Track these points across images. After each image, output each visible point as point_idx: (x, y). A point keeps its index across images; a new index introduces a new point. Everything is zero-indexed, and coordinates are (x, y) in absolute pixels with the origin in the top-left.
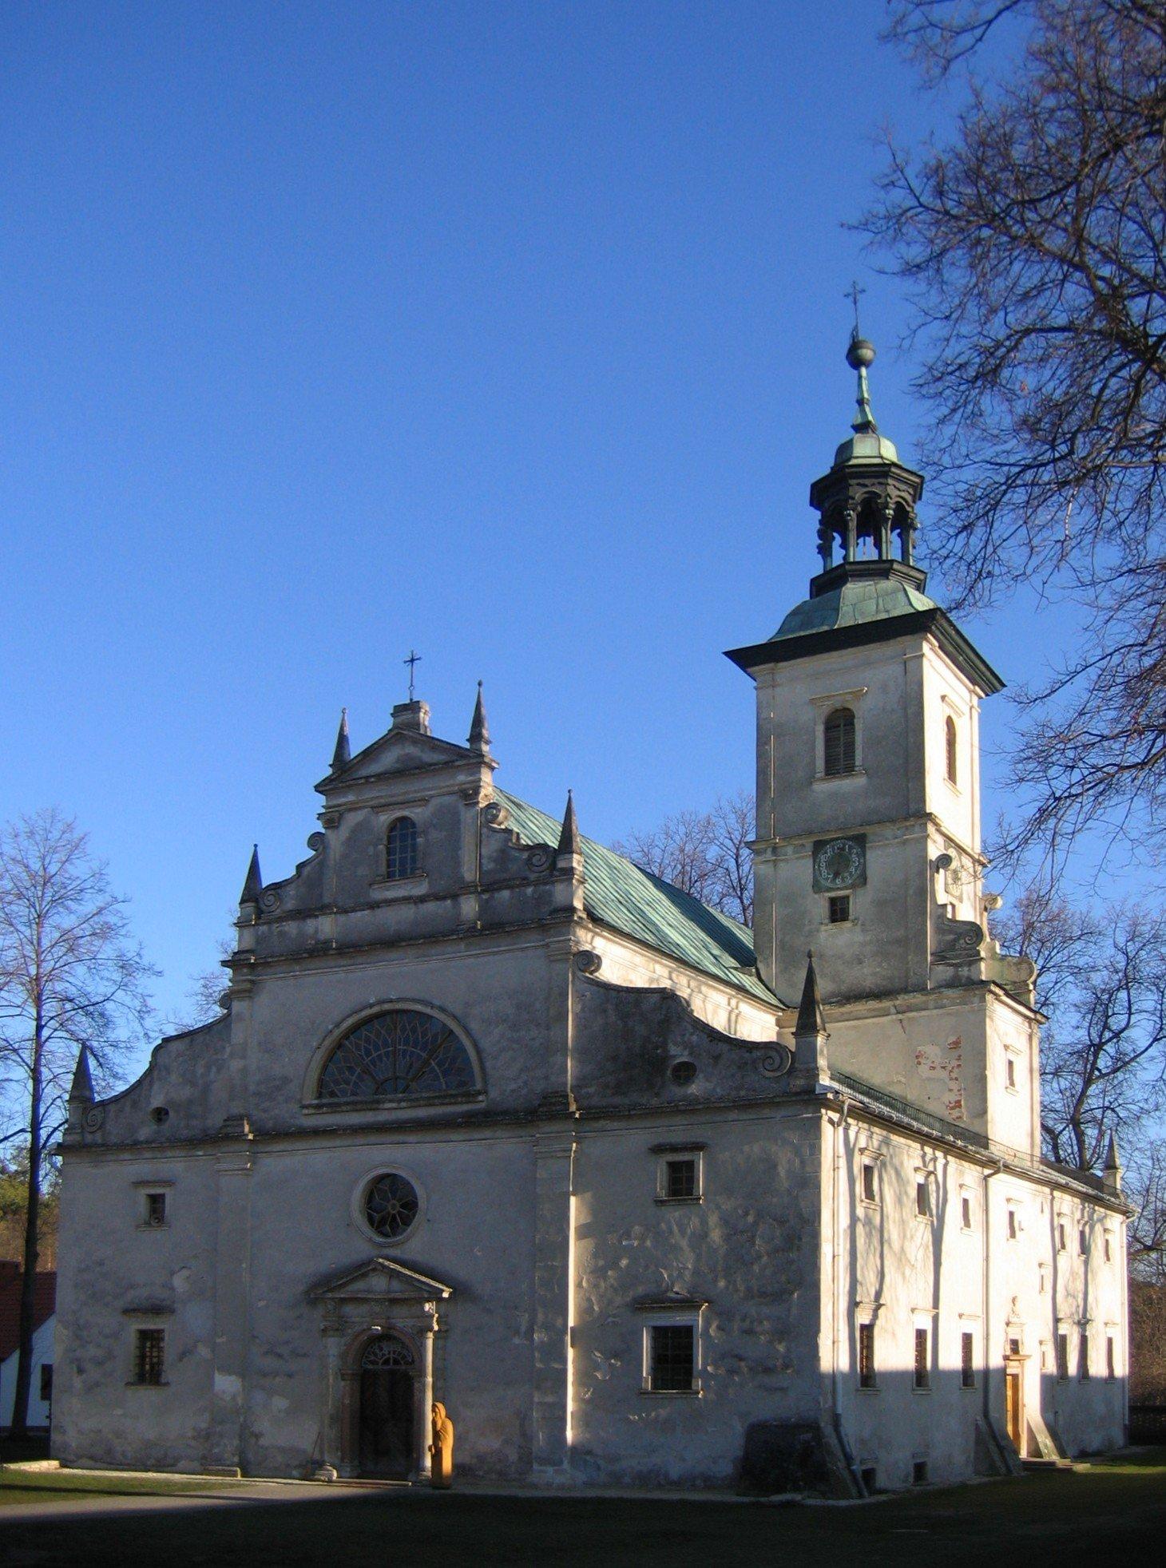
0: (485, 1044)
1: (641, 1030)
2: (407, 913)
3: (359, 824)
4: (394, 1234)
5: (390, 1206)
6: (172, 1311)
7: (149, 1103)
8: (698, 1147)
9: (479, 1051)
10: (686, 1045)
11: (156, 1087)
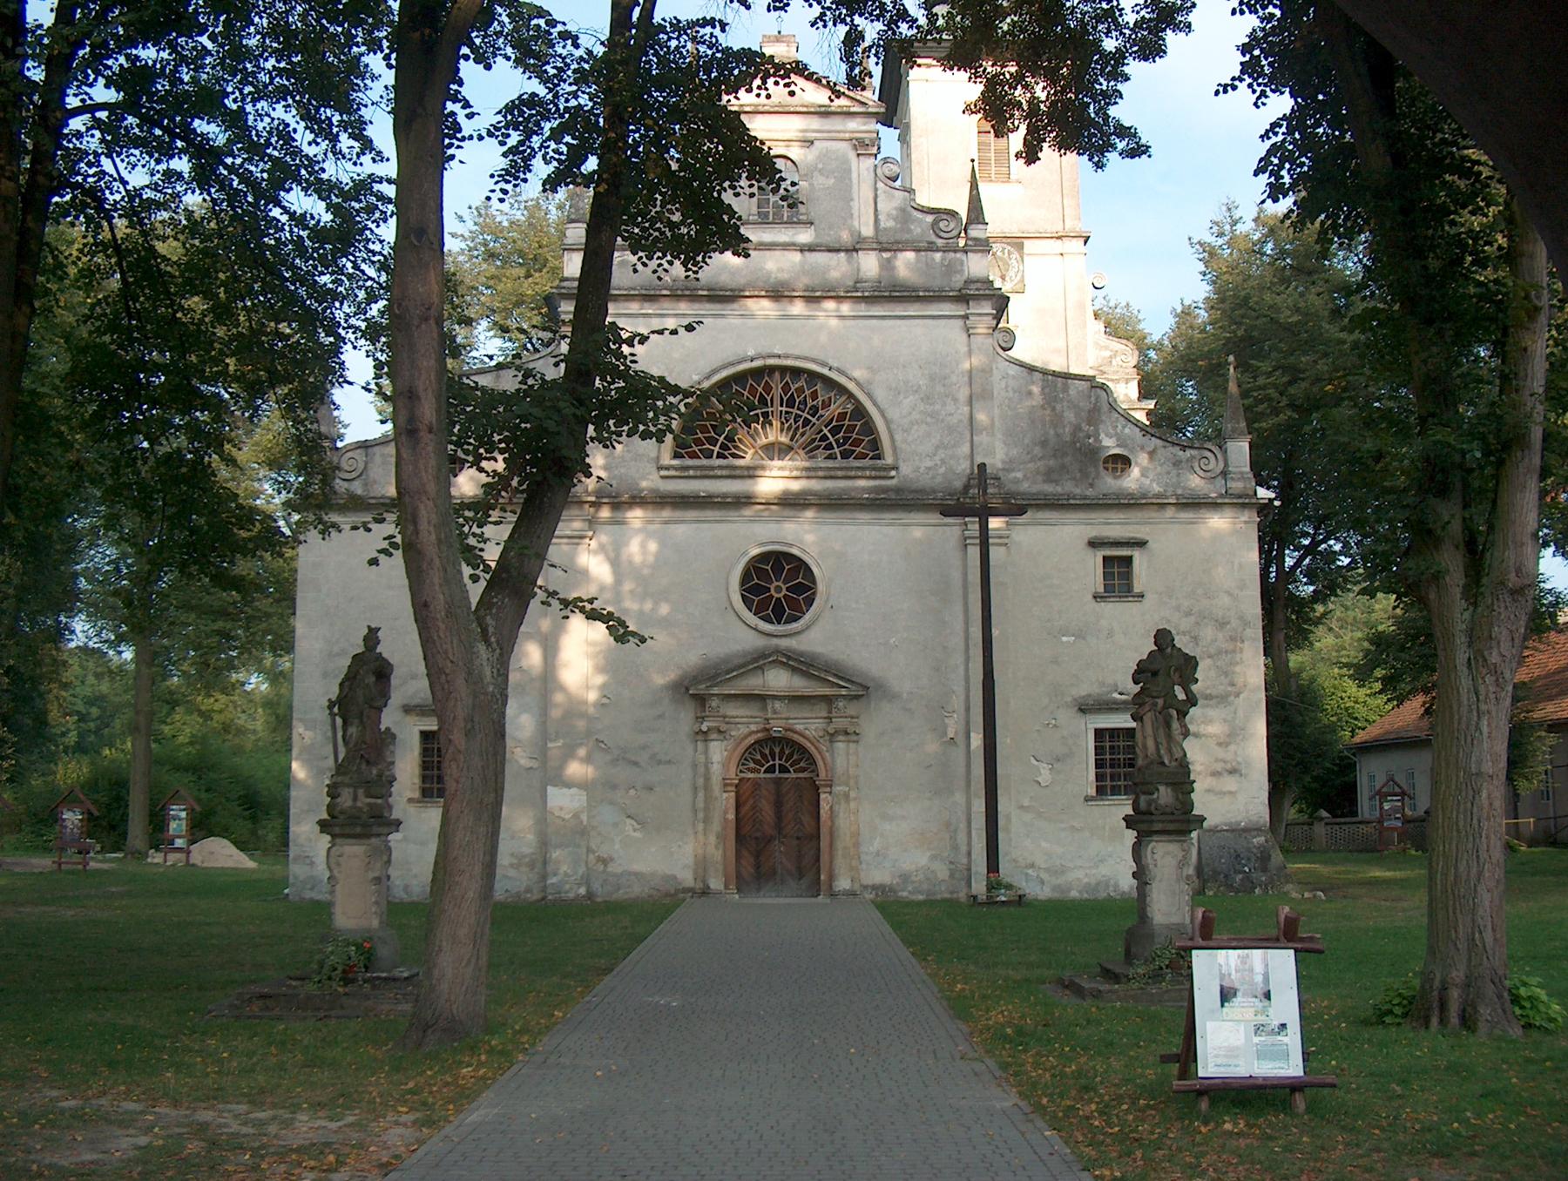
0: (893, 414)
8: (1141, 544)
9: (887, 422)
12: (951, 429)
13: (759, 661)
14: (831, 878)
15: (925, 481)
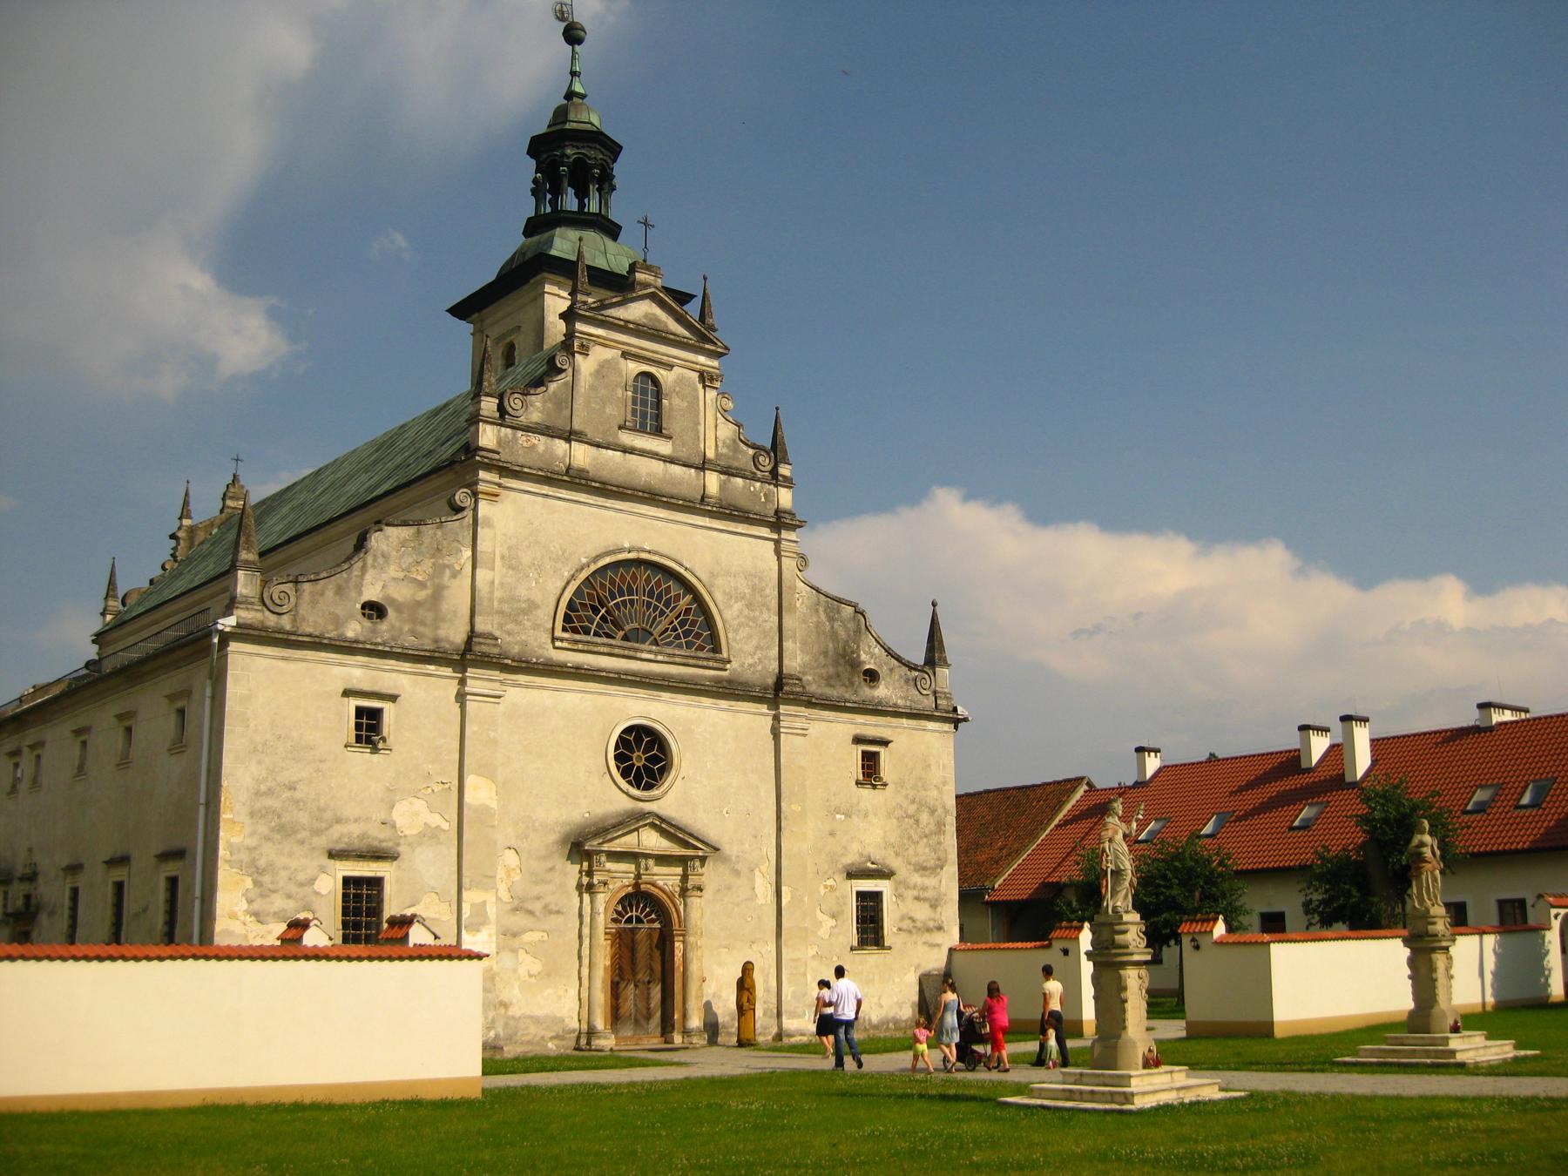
0: (728, 614)
1: (842, 634)
2: (658, 466)
3: (607, 361)
4: (649, 787)
5: (643, 757)
6: (395, 858)
7: (360, 593)
8: (885, 743)
10: (872, 655)
11: (368, 577)
12: (765, 634)
13: (631, 821)
14: (685, 1016)
15: (748, 676)
